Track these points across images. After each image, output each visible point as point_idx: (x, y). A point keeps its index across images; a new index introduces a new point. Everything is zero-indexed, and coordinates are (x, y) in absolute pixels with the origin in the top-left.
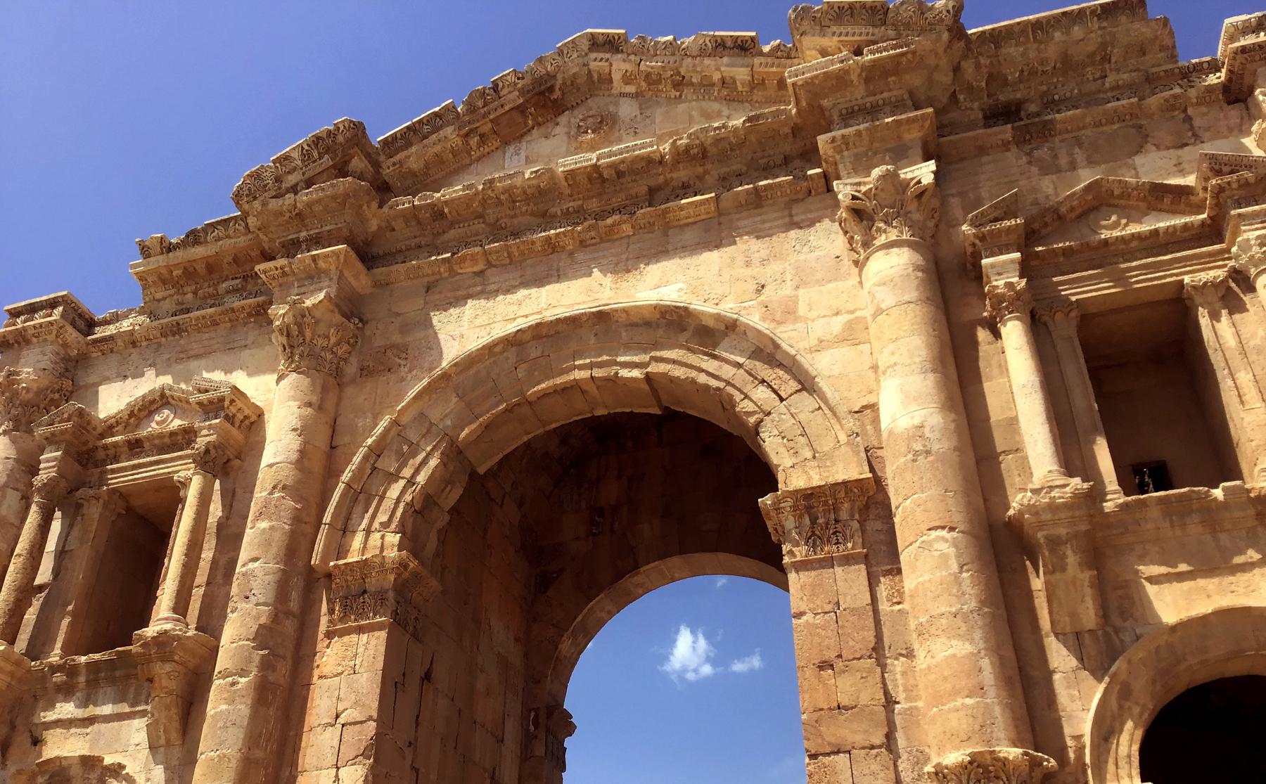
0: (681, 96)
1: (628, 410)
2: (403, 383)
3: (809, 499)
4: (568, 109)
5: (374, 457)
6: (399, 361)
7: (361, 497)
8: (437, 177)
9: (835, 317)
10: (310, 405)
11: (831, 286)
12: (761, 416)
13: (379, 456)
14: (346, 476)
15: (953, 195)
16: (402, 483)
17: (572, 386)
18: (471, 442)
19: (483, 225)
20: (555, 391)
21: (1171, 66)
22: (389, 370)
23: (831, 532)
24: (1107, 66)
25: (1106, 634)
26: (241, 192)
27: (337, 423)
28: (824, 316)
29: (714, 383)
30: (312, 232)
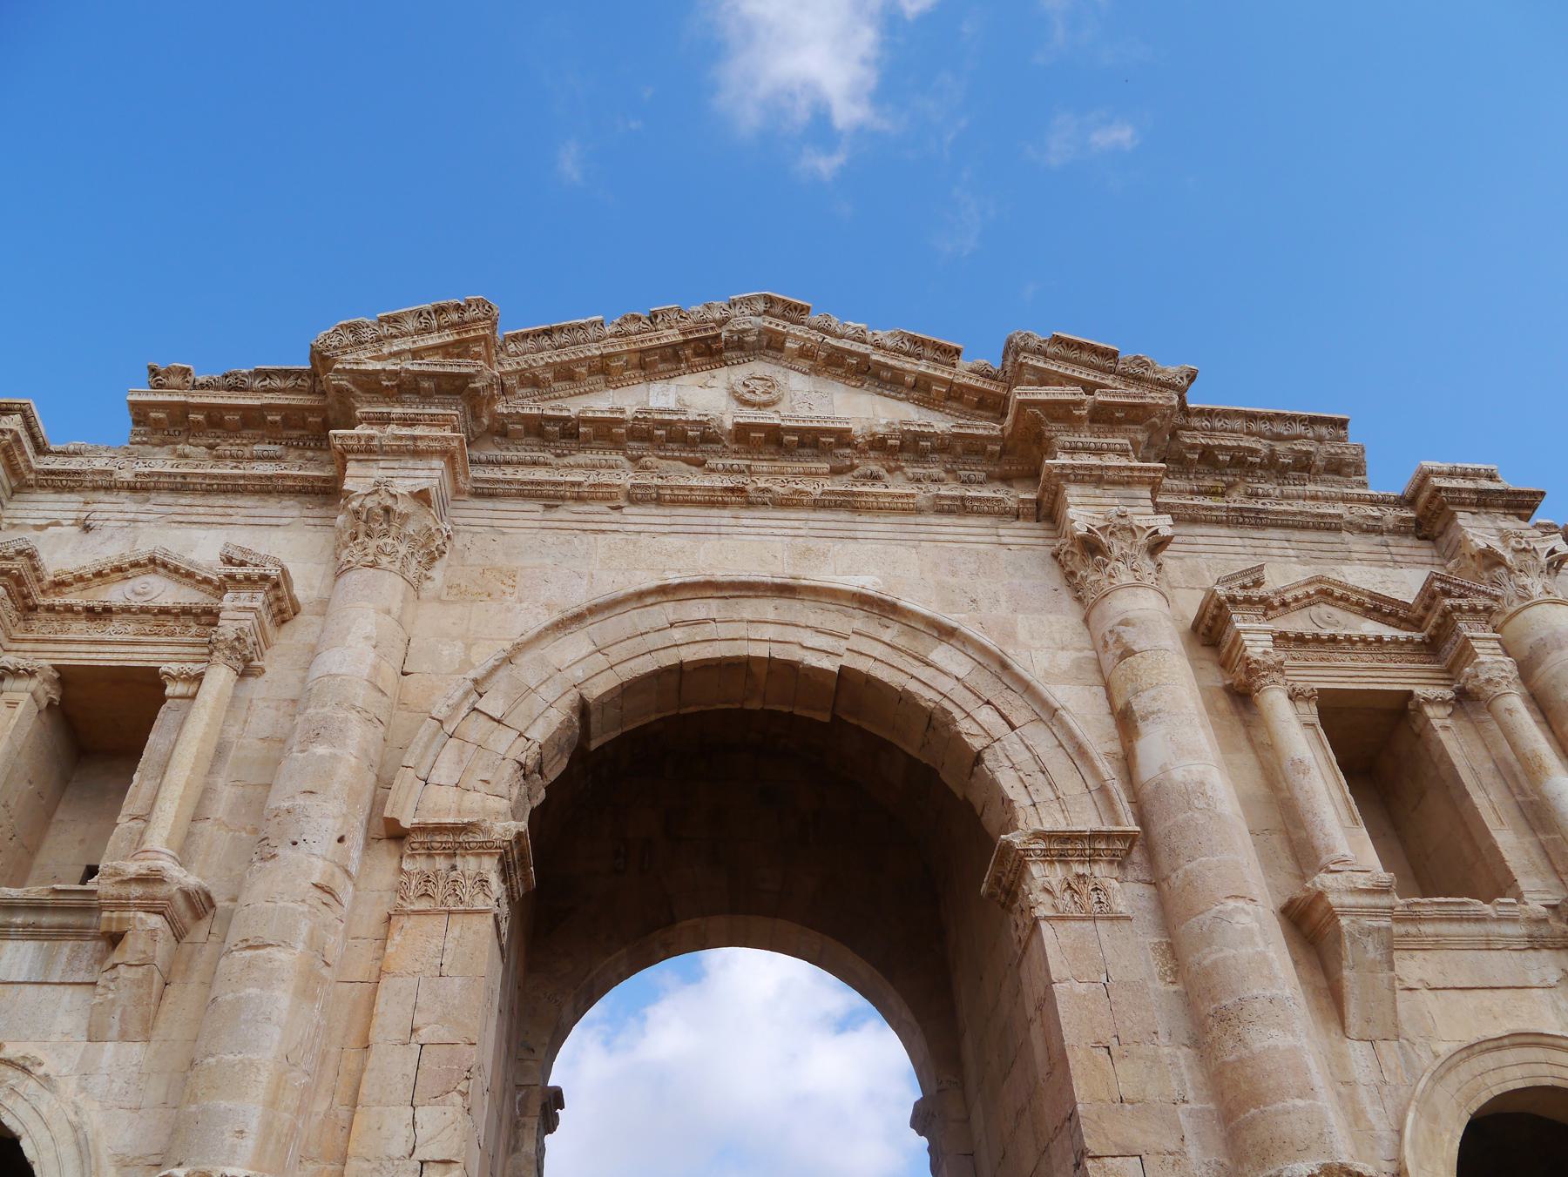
1: (786, 709)
2: (509, 615)
3: (1063, 845)
4: (727, 365)
6: (503, 587)
8: (562, 393)
10: (388, 612)
11: (1052, 618)
12: (986, 742)
16: (515, 734)
17: (740, 664)
19: (622, 458)
20: (717, 665)
22: (489, 595)
23: (1090, 888)
25: (1401, 1047)
26: (328, 341)
28: (1049, 648)
29: (927, 696)
30: (410, 411)
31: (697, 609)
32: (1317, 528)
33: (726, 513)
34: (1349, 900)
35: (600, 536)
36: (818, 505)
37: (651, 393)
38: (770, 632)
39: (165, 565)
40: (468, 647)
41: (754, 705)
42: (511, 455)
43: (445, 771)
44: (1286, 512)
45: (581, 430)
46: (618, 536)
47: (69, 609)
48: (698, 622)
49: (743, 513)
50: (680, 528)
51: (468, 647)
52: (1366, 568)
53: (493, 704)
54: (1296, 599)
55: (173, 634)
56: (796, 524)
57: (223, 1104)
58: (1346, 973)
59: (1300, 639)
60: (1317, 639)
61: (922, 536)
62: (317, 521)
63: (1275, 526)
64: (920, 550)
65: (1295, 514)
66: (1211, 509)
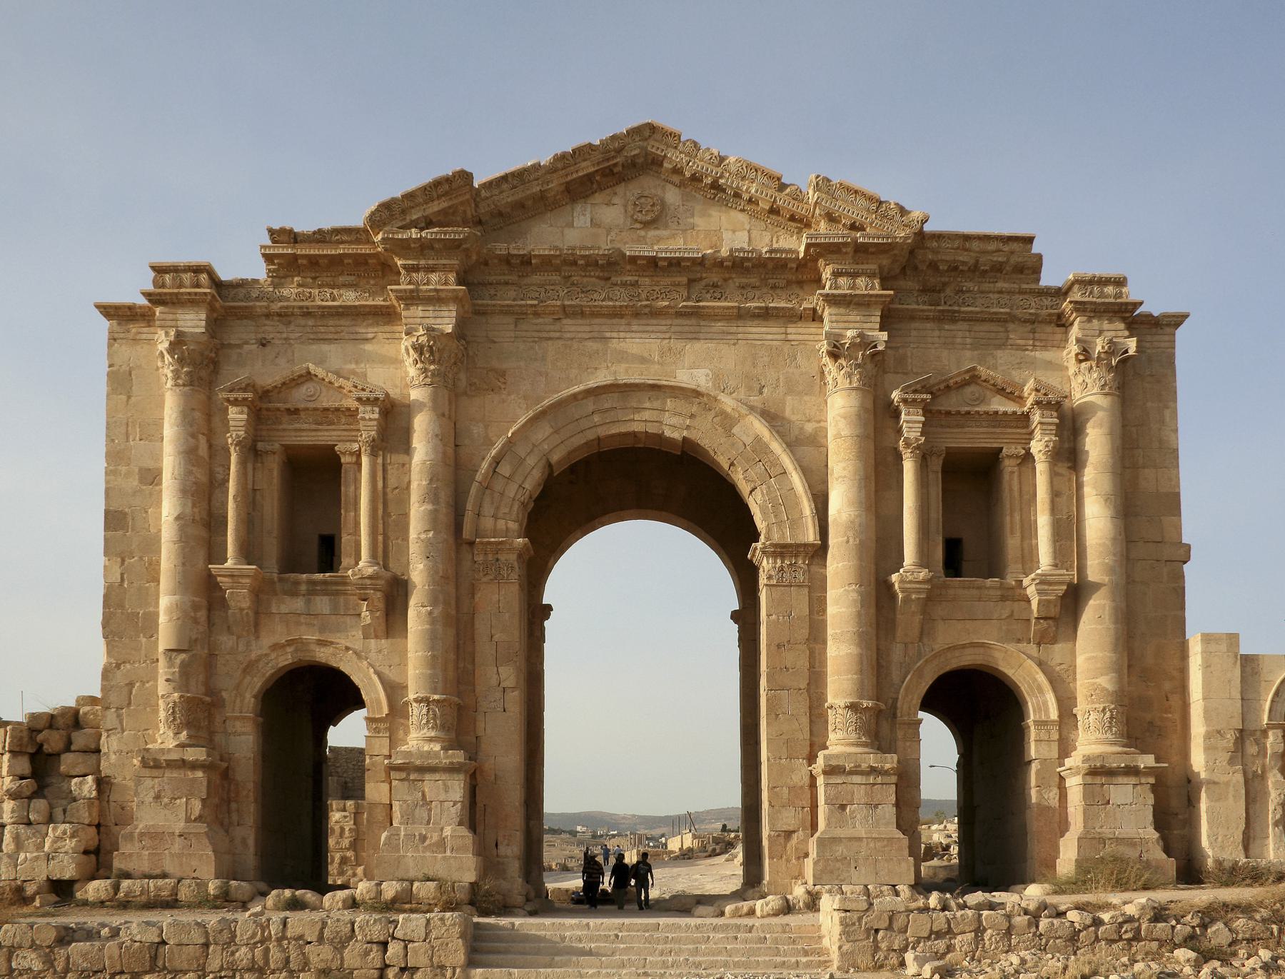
0: (714, 198)
2: (505, 404)
4: (624, 180)
5: (495, 464)
6: (499, 384)
7: (488, 492)
8: (518, 219)
9: (807, 423)
10: (443, 415)
11: (806, 398)
13: (498, 463)
14: (479, 477)
15: (890, 348)
16: (516, 486)
18: (559, 462)
19: (559, 278)
21: (1033, 286)
22: (492, 390)
24: (999, 275)
27: (457, 426)
31: (608, 402)
32: (992, 321)
33: (623, 321)
34: (909, 586)
35: (550, 343)
36: (680, 314)
37: (575, 214)
38: (646, 415)
39: (316, 376)
40: (486, 427)
41: (641, 445)
42: (492, 279)
43: (488, 509)
44: (971, 312)
45: (533, 262)
46: (561, 342)
47: (278, 409)
48: (607, 410)
49: (635, 322)
50: (596, 335)
51: (486, 427)
52: (1013, 352)
53: (505, 469)
54: (956, 383)
55: (332, 423)
56: (664, 328)
57: (429, 672)
58: (898, 616)
59: (948, 413)
60: (958, 413)
61: (740, 336)
62: (388, 335)
63: (964, 320)
64: (737, 346)
65: (977, 313)
66: (923, 311)
